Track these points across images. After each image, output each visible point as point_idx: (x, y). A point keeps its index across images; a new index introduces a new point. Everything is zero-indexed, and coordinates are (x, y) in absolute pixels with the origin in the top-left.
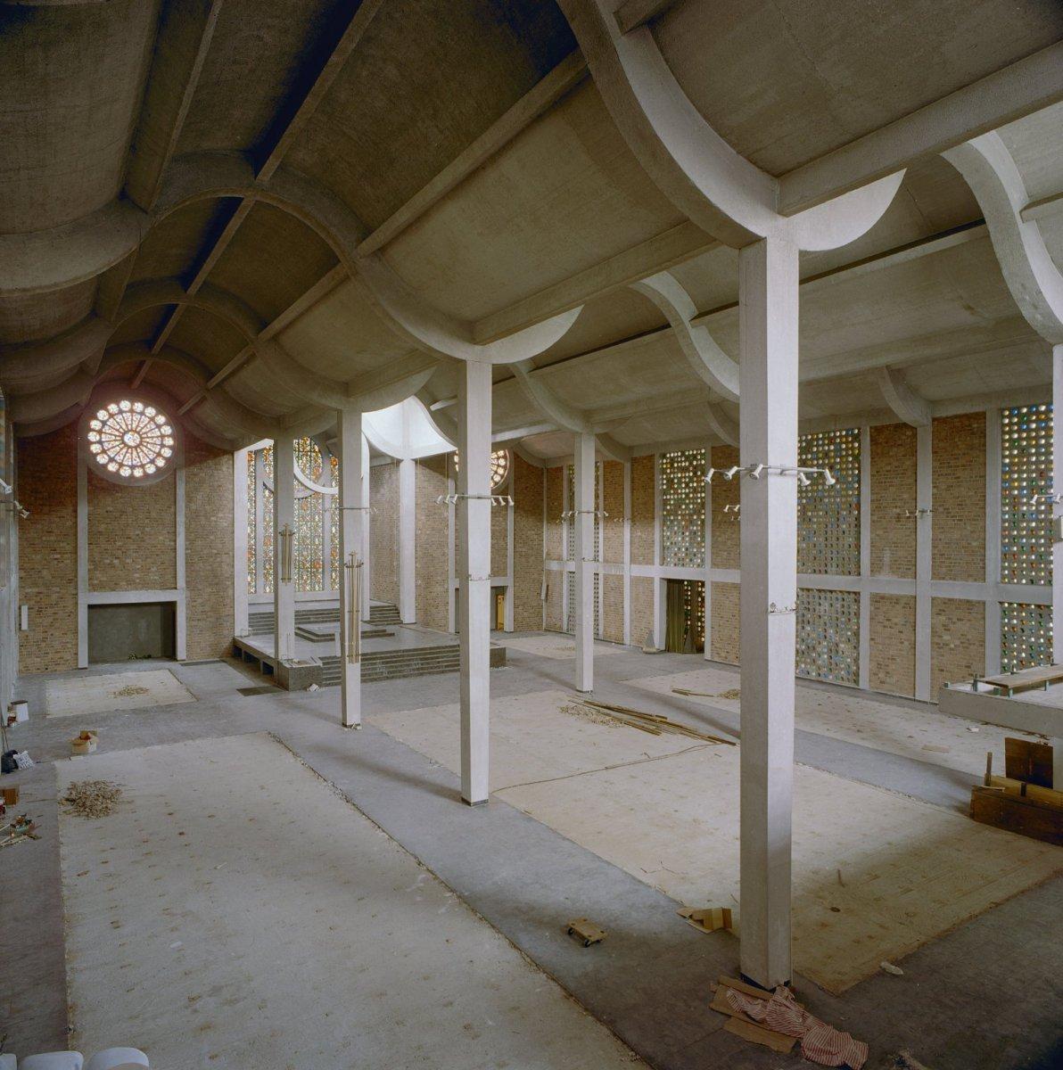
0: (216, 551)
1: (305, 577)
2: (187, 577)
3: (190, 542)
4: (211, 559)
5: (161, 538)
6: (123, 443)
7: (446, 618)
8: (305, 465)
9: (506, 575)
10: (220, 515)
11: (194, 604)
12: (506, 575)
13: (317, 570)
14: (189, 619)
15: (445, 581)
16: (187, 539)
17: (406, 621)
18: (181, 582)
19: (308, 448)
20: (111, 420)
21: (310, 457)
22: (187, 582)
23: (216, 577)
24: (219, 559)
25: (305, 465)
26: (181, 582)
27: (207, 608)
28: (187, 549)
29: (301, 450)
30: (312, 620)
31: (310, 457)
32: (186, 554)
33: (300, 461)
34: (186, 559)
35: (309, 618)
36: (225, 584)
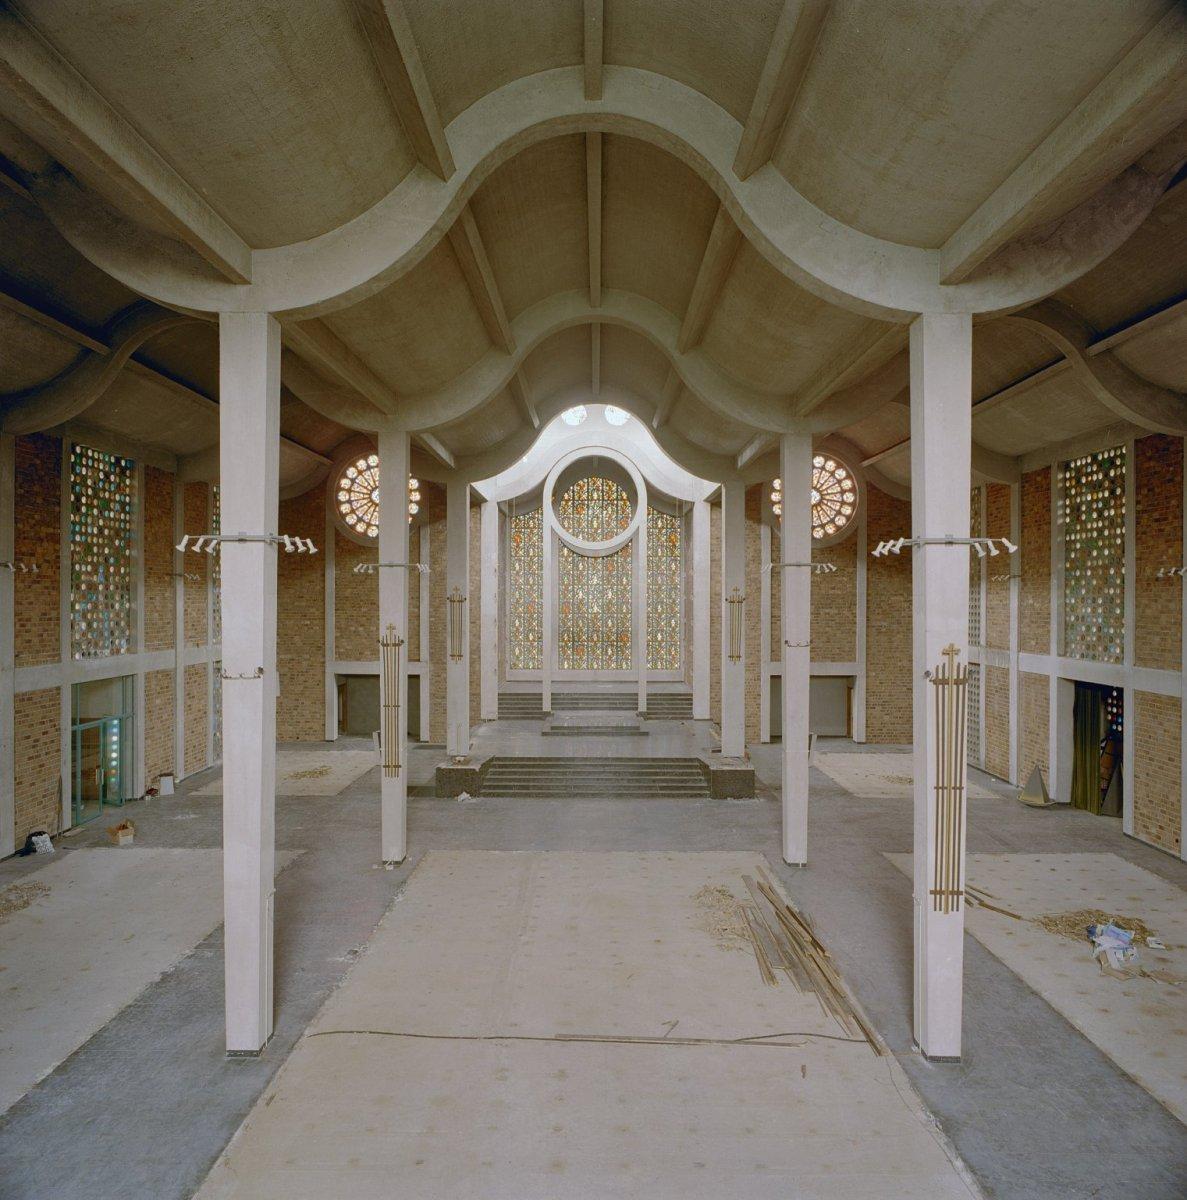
1: (610, 652)
6: (371, 501)
13: (625, 644)
16: (431, 605)
17: (696, 716)
19: (614, 496)
20: (360, 477)
28: (431, 617)
30: (580, 705)
33: (605, 512)
34: (431, 629)
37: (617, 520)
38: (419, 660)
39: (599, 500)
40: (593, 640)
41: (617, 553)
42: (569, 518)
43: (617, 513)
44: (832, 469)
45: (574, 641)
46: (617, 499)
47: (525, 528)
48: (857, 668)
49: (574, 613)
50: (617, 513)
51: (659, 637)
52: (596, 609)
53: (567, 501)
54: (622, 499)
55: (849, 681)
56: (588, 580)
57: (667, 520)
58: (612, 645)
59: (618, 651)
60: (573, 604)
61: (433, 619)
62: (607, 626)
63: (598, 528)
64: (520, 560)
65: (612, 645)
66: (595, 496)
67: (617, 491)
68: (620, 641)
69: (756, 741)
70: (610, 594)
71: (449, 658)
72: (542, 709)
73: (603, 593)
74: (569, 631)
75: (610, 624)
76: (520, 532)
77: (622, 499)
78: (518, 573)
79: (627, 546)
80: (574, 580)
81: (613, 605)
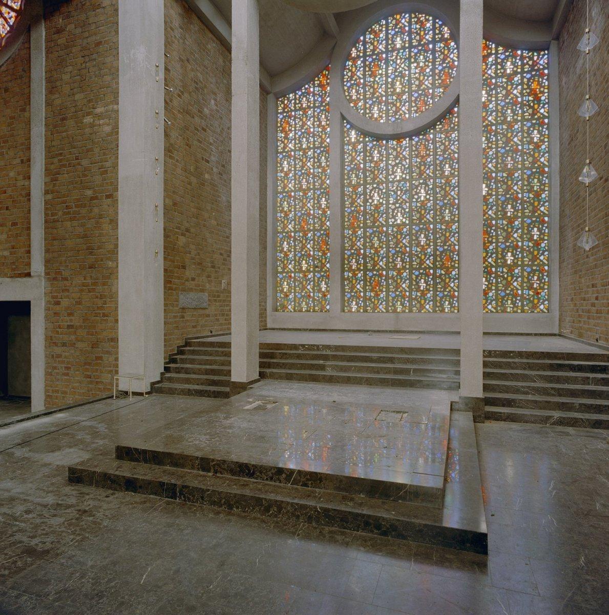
0: (89, 193)
1: (423, 285)
2: (47, 251)
3: (52, 175)
4: (84, 211)
5: (12, 174)
8: (422, 70)
10: (99, 110)
11: (57, 308)
13: (448, 273)
14: (50, 341)
18: (37, 265)
21: (434, 51)
22: (47, 262)
23: (90, 250)
24: (96, 210)
25: (422, 70)
26: (37, 265)
27: (76, 321)
28: (47, 192)
29: (415, 43)
30: (329, 372)
31: (434, 51)
32: (46, 203)
33: (413, 66)
34: (46, 215)
35: (322, 368)
36: (108, 268)
37: (433, 75)
38: (28, 275)
39: (404, 48)
40: (395, 268)
41: (432, 125)
42: (358, 85)
45: (366, 270)
46: (434, 41)
47: (296, 110)
49: (365, 227)
50: (434, 63)
51: (509, 258)
52: (400, 219)
53: (354, 60)
54: (442, 40)
56: (387, 174)
57: (522, 58)
58: (427, 275)
59: (435, 284)
60: (365, 213)
61: (49, 197)
62: (418, 245)
63: (403, 92)
64: (290, 156)
65: (427, 275)
66: (398, 43)
67: (434, 28)
68: (440, 269)
72: (229, 373)
73: (412, 191)
74: (359, 254)
76: (290, 117)
77: (442, 40)
78: (287, 174)
79: (449, 111)
80: (365, 177)
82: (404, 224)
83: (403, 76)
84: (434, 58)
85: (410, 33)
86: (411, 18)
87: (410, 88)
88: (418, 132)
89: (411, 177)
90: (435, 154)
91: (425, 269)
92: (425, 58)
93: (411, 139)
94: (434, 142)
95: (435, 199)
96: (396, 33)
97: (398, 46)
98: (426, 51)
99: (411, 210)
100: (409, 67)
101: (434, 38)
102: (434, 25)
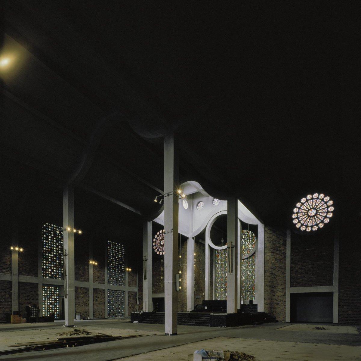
1: (248, 294)
7: (284, 310)
9: (332, 284)
12: (332, 284)
13: (254, 291)
15: (284, 289)
19: (250, 236)
21: (251, 239)
29: (247, 237)
31: (251, 239)
33: (247, 242)
39: (244, 238)
41: (250, 257)
43: (251, 242)
44: (311, 197)
46: (251, 237)
48: (334, 289)
50: (251, 242)
54: (253, 237)
55: (331, 294)
65: (249, 291)
69: (284, 321)
70: (248, 273)
71: (143, 280)
73: (246, 272)
75: (248, 283)
77: (253, 237)
81: (249, 276)
82: (244, 280)
83: (244, 245)
84: (251, 241)
85: (246, 235)
86: (246, 231)
87: (246, 248)
88: (247, 258)
89: (246, 269)
90: (251, 263)
91: (249, 290)
92: (249, 241)
93: (246, 260)
94: (251, 260)
95: (251, 274)
96: (243, 235)
97: (243, 238)
98: (249, 239)
99: (246, 276)
100: (246, 243)
101: (251, 236)
102: (251, 233)
